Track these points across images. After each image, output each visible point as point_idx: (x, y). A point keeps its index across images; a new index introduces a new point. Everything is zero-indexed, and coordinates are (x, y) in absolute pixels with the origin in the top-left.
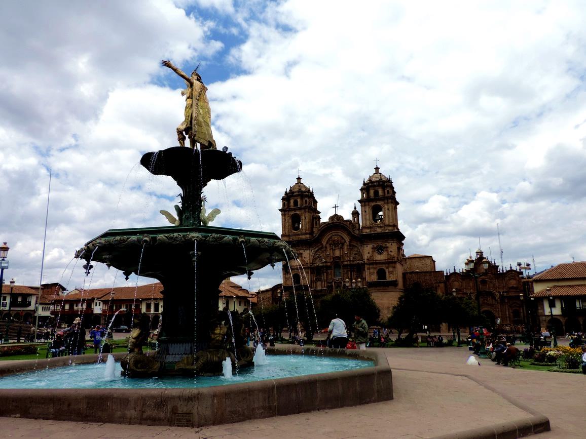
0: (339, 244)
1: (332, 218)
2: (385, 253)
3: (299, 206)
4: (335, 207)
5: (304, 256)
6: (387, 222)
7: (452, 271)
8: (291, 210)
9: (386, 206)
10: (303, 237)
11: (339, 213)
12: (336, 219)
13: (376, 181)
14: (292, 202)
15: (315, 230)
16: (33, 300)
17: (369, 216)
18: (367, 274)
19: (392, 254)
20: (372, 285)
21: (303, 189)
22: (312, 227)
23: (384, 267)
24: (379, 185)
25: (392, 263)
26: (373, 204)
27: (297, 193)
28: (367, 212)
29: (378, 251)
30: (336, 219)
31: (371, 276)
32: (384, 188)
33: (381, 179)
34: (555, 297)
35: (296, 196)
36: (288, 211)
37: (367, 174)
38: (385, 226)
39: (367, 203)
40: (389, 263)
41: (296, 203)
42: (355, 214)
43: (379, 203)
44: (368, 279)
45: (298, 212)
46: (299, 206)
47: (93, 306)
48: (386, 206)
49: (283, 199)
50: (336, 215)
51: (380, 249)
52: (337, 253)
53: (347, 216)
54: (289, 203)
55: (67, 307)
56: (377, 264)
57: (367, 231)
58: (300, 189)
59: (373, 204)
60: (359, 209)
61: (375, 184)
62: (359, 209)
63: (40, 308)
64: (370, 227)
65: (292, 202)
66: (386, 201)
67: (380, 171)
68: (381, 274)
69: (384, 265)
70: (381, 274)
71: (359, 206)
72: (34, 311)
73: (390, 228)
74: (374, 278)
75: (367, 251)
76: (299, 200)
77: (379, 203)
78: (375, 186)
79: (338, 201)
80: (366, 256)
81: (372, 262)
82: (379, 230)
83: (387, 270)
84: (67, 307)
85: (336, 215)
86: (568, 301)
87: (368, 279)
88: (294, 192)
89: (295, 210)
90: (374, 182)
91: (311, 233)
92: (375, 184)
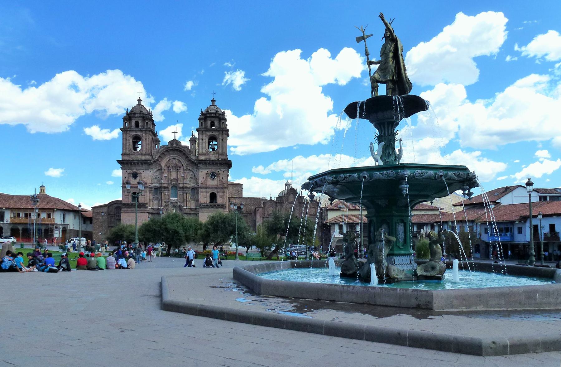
0: (177, 167)
1: (171, 142)
3: (140, 127)
4: (175, 132)
5: (143, 175)
6: (220, 151)
7: (269, 199)
8: (132, 130)
9: (221, 137)
10: (144, 157)
11: (177, 139)
13: (213, 113)
19: (223, 180)
21: (145, 112)
23: (215, 191)
24: (215, 117)
25: (222, 188)
26: (209, 133)
27: (138, 115)
28: (204, 140)
29: (212, 176)
31: (204, 199)
33: (217, 112)
35: (138, 117)
36: (129, 131)
38: (218, 155)
39: (204, 132)
40: (220, 188)
41: (137, 125)
45: (139, 133)
46: (140, 127)
48: (221, 137)
50: (175, 140)
51: (213, 175)
52: (174, 176)
54: (130, 123)
56: (209, 188)
57: (202, 158)
58: (141, 111)
61: (212, 115)
64: (206, 155)
65: (133, 123)
66: (221, 132)
67: (216, 103)
68: (213, 197)
69: (216, 190)
70: (213, 197)
71: (196, 135)
73: (223, 157)
75: (202, 174)
76: (140, 122)
78: (212, 117)
80: (201, 181)
83: (218, 195)
85: (175, 140)
88: (135, 113)
89: (136, 131)
90: (211, 113)
92: (212, 115)
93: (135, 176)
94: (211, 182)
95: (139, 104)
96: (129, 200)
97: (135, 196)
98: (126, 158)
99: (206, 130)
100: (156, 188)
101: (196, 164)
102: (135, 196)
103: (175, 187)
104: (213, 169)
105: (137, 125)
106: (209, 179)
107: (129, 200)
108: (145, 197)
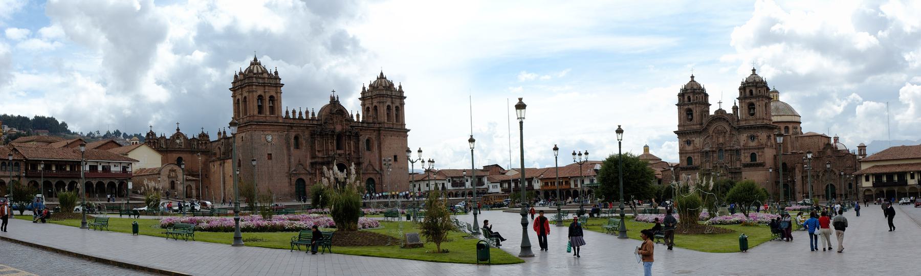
1: (716, 112)
2: (756, 141)
8: (685, 105)
12: (720, 112)
14: (686, 97)
15: (704, 121)
16: (485, 180)
17: (746, 110)
18: (742, 157)
20: (746, 166)
21: (695, 87)
22: (702, 119)
23: (755, 151)
26: (748, 101)
30: (720, 112)
31: (745, 158)
32: (757, 87)
34: (914, 172)
37: (745, 74)
42: (735, 108)
43: (753, 100)
44: (743, 161)
45: (690, 107)
47: (533, 183)
49: (679, 95)
50: (720, 109)
51: (752, 138)
52: (721, 140)
53: (729, 111)
55: (513, 185)
57: (743, 123)
59: (748, 101)
60: (738, 104)
62: (738, 104)
63: (491, 186)
65: (686, 97)
68: (753, 156)
70: (753, 156)
71: (737, 101)
72: (487, 189)
74: (748, 160)
75: (743, 138)
77: (753, 100)
79: (723, 97)
81: (746, 148)
82: (752, 123)
84: (513, 185)
85: (720, 109)
86: (878, 176)
87: (743, 161)
91: (701, 124)
93: (689, 143)
94: (753, 144)
95: (693, 81)
96: (685, 164)
97: (689, 160)
98: (682, 128)
99: (745, 98)
100: (707, 152)
101: (740, 129)
102: (689, 160)
103: (720, 150)
104: (752, 132)
105: (689, 99)
106: (750, 141)
107: (685, 164)
108: (697, 160)
